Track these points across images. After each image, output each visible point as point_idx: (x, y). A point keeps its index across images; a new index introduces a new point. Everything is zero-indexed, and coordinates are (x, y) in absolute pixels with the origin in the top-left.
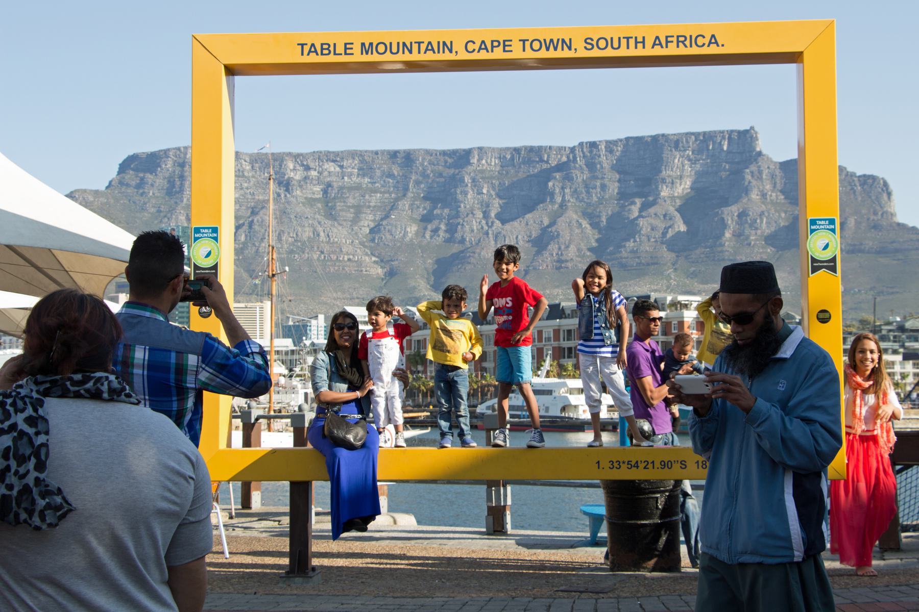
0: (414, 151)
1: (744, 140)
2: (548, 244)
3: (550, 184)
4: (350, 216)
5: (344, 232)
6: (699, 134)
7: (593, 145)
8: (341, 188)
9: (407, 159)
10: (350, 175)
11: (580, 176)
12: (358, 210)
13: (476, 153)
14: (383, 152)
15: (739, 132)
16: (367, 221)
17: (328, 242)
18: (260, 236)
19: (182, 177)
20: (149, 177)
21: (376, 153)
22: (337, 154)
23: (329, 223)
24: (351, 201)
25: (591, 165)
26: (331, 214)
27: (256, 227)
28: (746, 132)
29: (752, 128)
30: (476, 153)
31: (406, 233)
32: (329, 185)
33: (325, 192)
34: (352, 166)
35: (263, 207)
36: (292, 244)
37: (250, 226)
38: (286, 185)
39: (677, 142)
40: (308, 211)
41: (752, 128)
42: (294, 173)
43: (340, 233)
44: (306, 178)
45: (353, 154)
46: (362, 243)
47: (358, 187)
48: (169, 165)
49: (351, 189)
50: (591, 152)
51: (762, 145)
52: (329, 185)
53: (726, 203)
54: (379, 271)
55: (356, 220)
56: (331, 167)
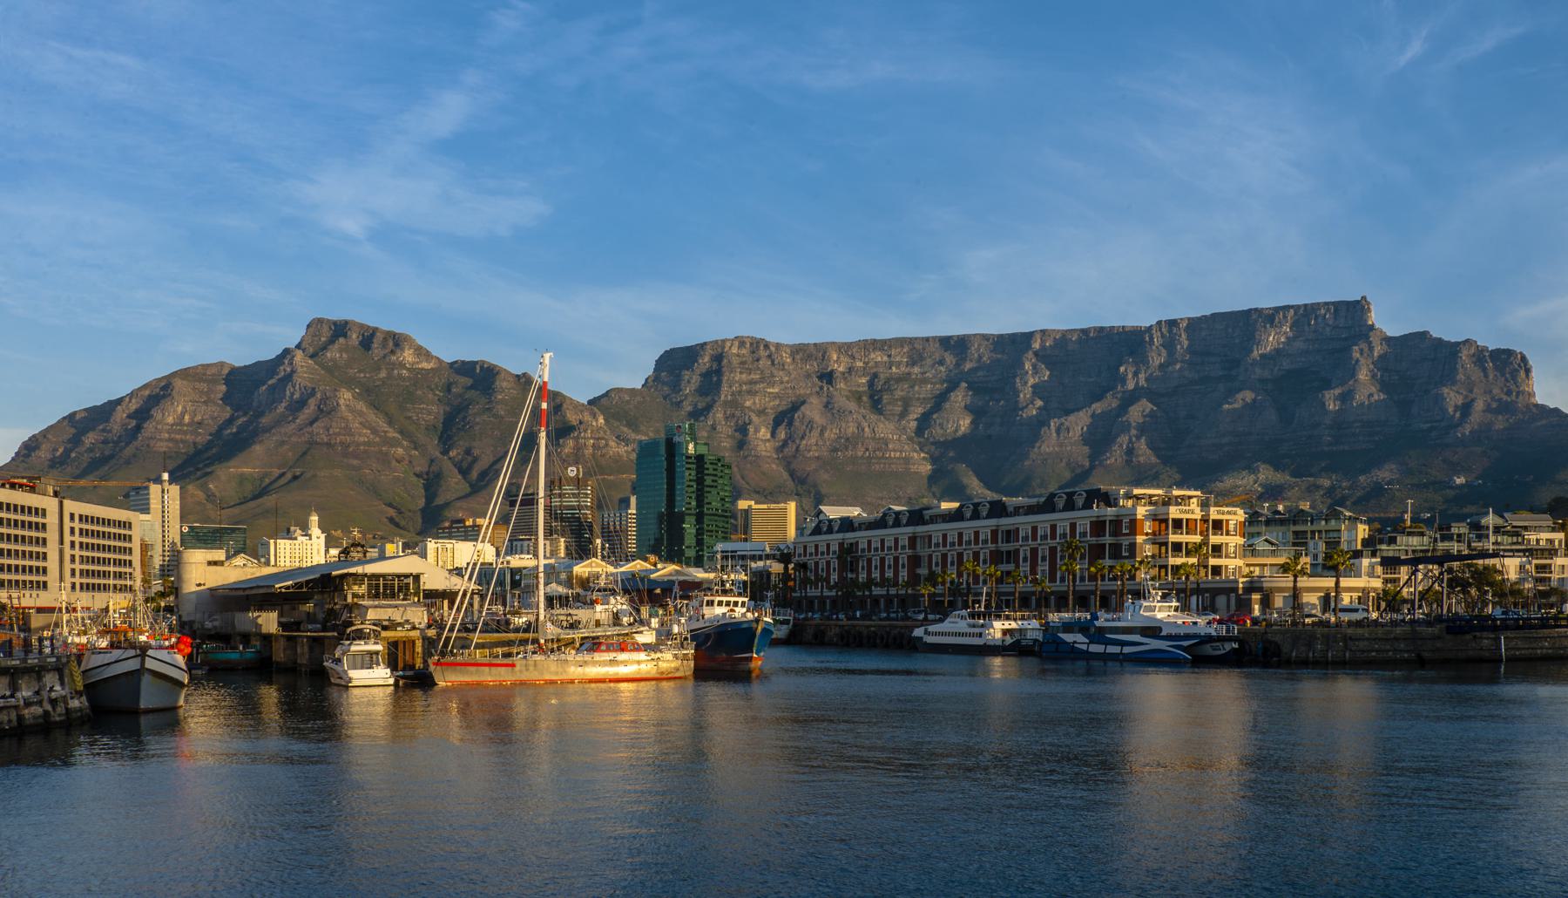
0: (969, 336)
1: (1358, 308)
2: (1118, 435)
3: (1122, 369)
4: (898, 409)
5: (891, 426)
6: (1299, 307)
7: (1172, 323)
8: (887, 381)
9: (957, 345)
10: (899, 364)
11: (1157, 358)
12: (907, 403)
13: (1038, 336)
14: (934, 338)
15: (1348, 303)
16: (917, 411)
17: (873, 438)
18: (800, 433)
19: (719, 372)
20: (686, 374)
21: (927, 339)
22: (884, 342)
23: (874, 417)
24: (899, 394)
25: (1169, 345)
26: (876, 405)
27: (797, 423)
28: (1358, 302)
29: (1364, 298)
30: (1038, 336)
31: (959, 426)
32: (875, 376)
33: (871, 384)
34: (900, 356)
35: (804, 403)
36: (835, 441)
37: (790, 424)
38: (828, 377)
39: (1270, 317)
40: (852, 406)
41: (1364, 298)
42: (838, 365)
43: (885, 429)
44: (850, 370)
45: (901, 342)
46: (910, 439)
47: (905, 378)
48: (705, 361)
49: (900, 379)
50: (1170, 331)
51: (1375, 317)
52: (875, 376)
53: (1327, 384)
54: (927, 468)
55: (903, 415)
56: (878, 357)
